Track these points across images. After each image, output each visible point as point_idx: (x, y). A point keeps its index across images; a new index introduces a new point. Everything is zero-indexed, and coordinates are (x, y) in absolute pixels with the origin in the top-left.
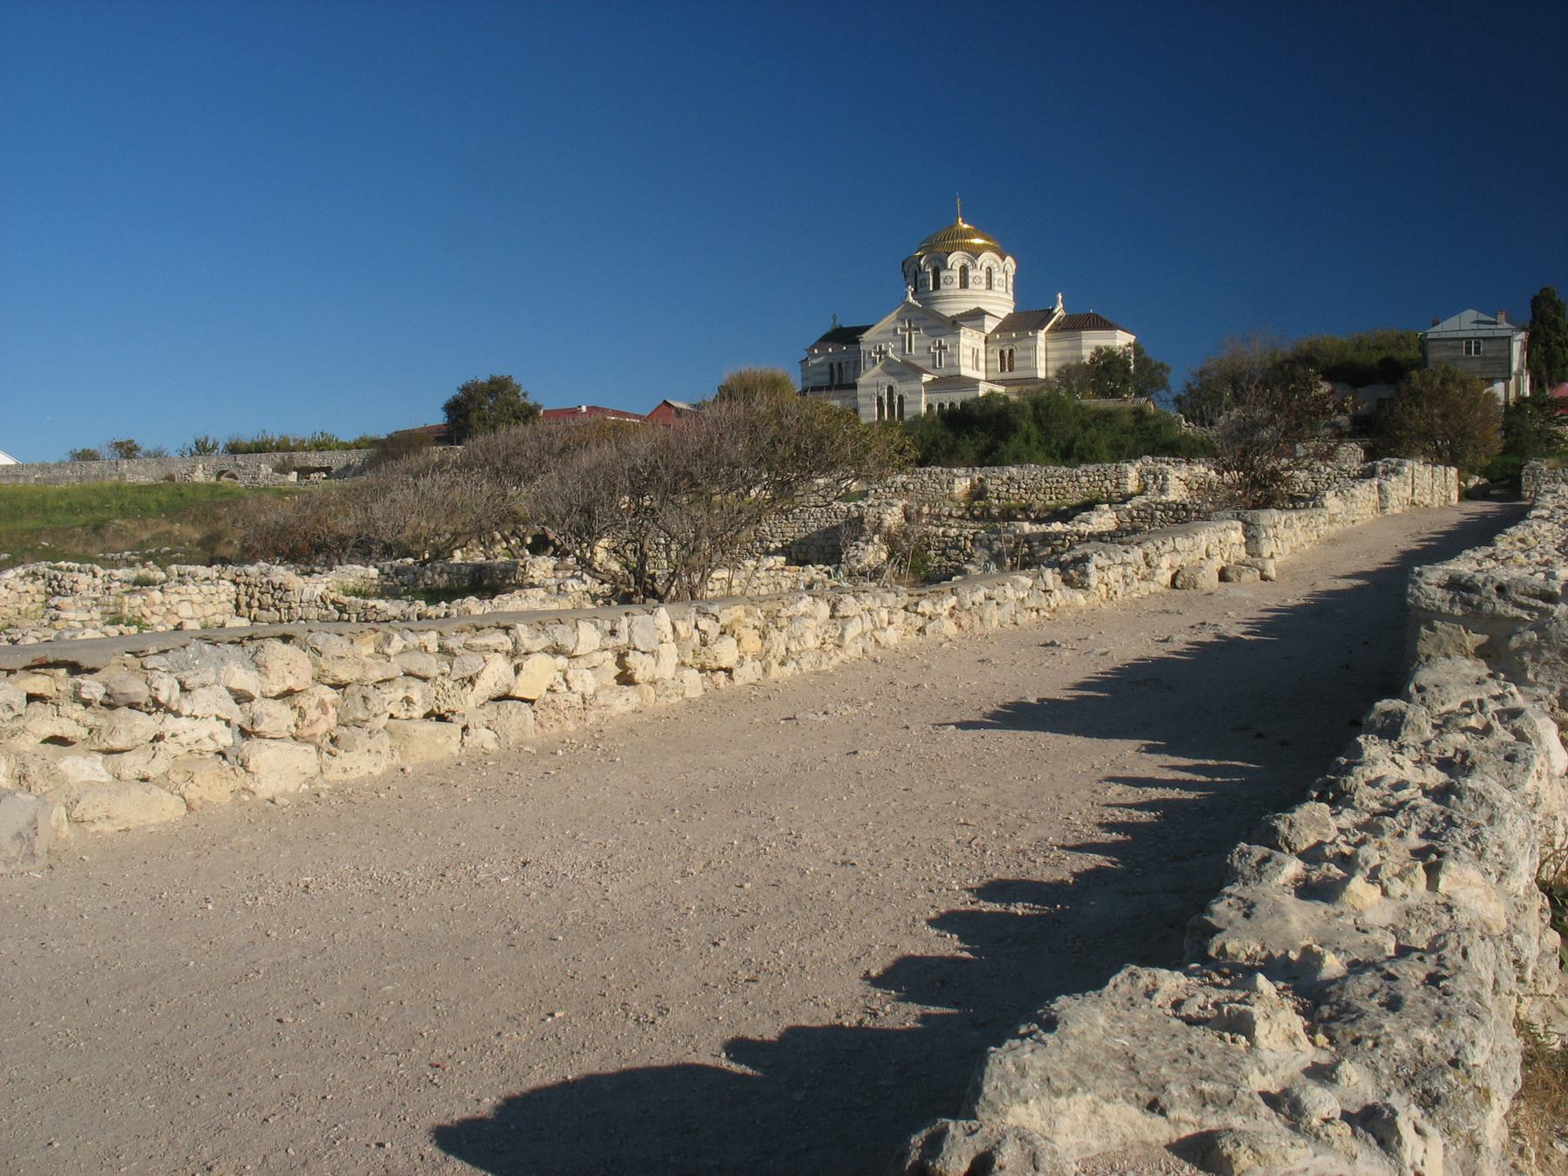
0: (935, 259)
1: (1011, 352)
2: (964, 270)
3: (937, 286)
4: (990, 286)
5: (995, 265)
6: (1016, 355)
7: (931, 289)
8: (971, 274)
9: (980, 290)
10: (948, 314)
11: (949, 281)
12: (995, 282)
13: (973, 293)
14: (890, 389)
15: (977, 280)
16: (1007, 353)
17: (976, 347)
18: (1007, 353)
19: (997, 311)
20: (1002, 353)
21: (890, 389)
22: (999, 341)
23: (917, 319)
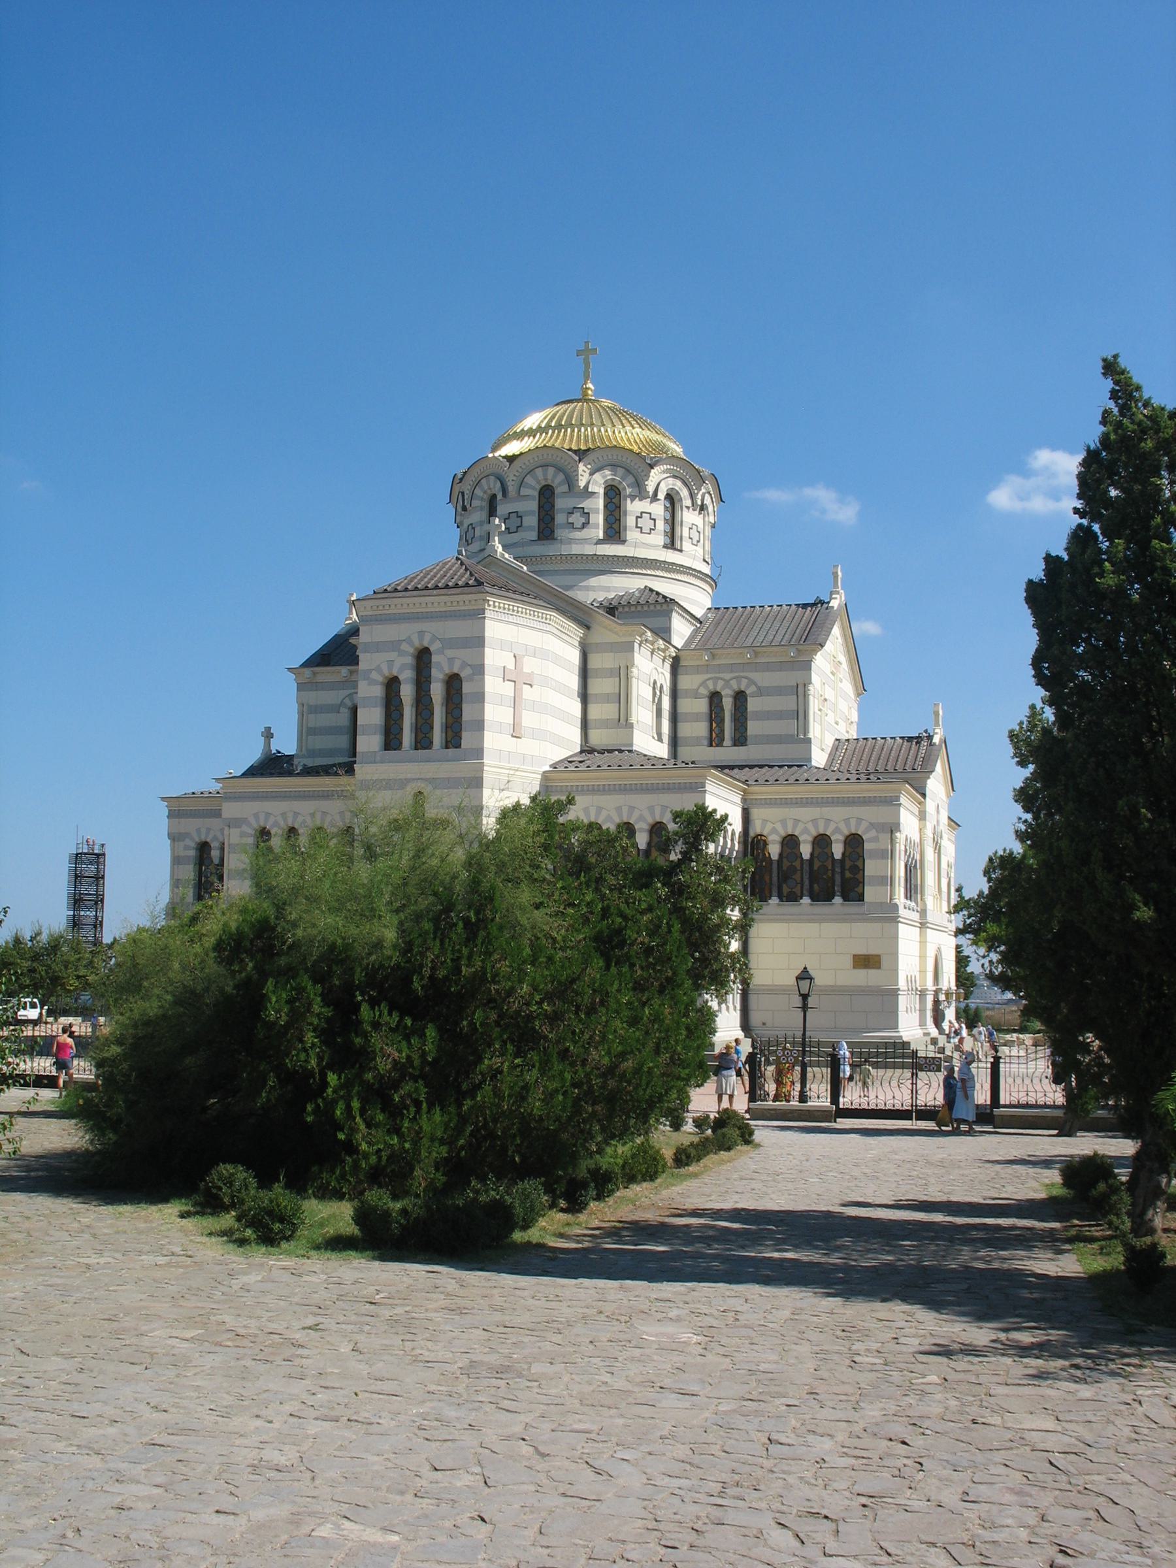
0: (544, 466)
1: (740, 698)
3: (546, 531)
4: (672, 543)
5: (684, 493)
6: (753, 705)
7: (534, 535)
8: (634, 507)
9: (655, 547)
11: (577, 519)
15: (646, 523)
16: (728, 704)
18: (728, 704)
19: (687, 599)
20: (715, 698)
22: (707, 668)
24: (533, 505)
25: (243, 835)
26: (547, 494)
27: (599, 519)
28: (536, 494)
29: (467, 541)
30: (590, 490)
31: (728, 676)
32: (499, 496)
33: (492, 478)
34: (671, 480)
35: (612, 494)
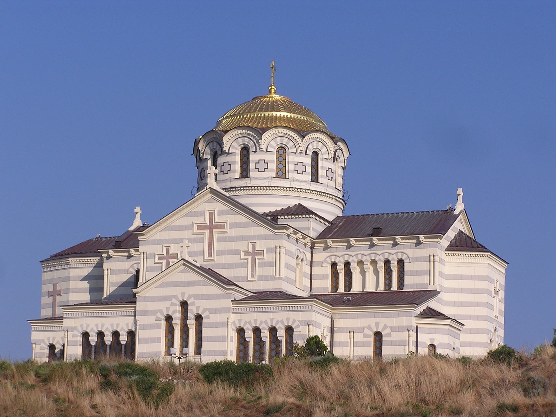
2: (282, 150)
3: (245, 173)
4: (315, 178)
7: (237, 175)
8: (292, 159)
10: (260, 210)
11: (262, 166)
12: (321, 172)
13: (296, 185)
14: (184, 305)
15: (300, 168)
16: (341, 268)
17: (301, 256)
21: (184, 305)
23: (221, 213)
24: (238, 158)
25: (74, 336)
26: (245, 151)
27: (273, 166)
28: (238, 152)
29: (201, 178)
30: (268, 150)
31: (339, 254)
32: (219, 153)
33: (215, 143)
34: (315, 143)
35: (281, 152)
